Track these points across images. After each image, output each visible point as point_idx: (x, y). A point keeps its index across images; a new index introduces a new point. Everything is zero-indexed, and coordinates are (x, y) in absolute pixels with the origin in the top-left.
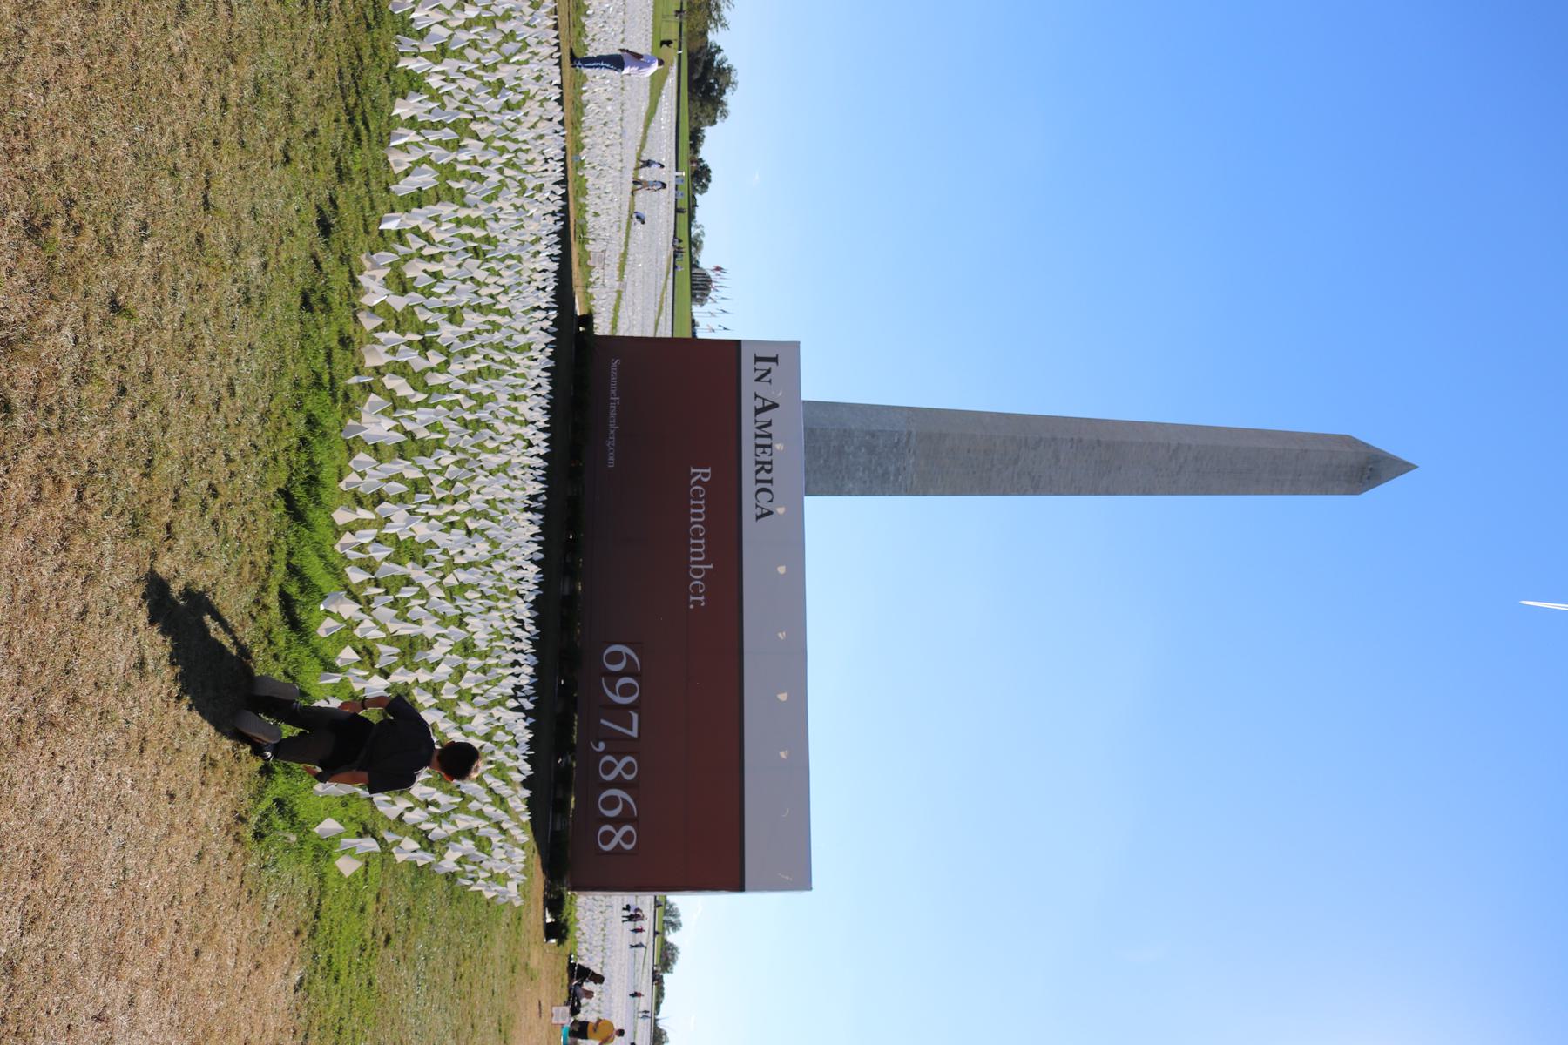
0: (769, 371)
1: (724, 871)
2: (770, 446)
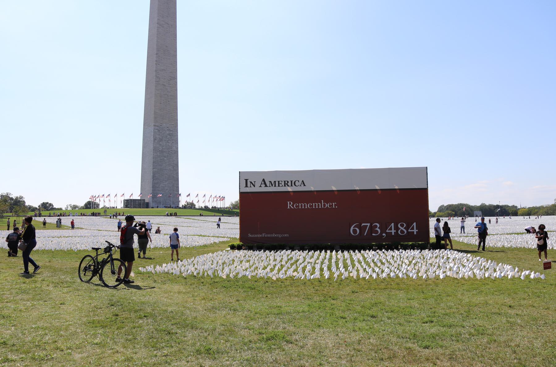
0: (251, 182)
2: (279, 182)
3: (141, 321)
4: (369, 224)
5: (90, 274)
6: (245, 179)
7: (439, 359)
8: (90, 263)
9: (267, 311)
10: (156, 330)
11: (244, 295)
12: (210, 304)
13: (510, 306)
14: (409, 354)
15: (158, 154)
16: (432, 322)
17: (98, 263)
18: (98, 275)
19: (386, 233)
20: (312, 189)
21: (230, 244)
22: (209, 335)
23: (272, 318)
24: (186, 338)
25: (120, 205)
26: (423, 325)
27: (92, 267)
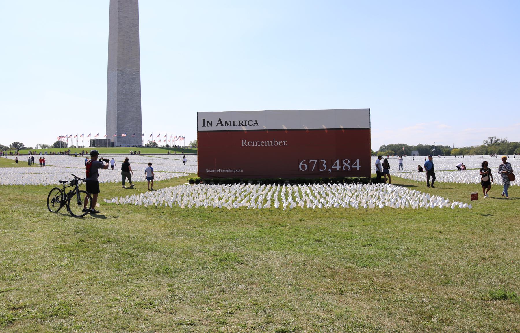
0: (208, 122)
1: (365, 134)
2: (234, 121)
3: (105, 246)
4: (316, 161)
5: (57, 205)
6: (203, 119)
7: (375, 276)
8: (58, 195)
9: (221, 236)
10: (119, 253)
11: (200, 223)
12: (169, 231)
13: (440, 232)
14: (349, 272)
15: (122, 97)
16: (370, 245)
17: (65, 195)
18: (65, 205)
19: (332, 169)
20: (265, 128)
21: (189, 179)
22: (167, 257)
23: (225, 242)
24: (146, 260)
25: (87, 145)
26: (363, 247)
27: (60, 199)
